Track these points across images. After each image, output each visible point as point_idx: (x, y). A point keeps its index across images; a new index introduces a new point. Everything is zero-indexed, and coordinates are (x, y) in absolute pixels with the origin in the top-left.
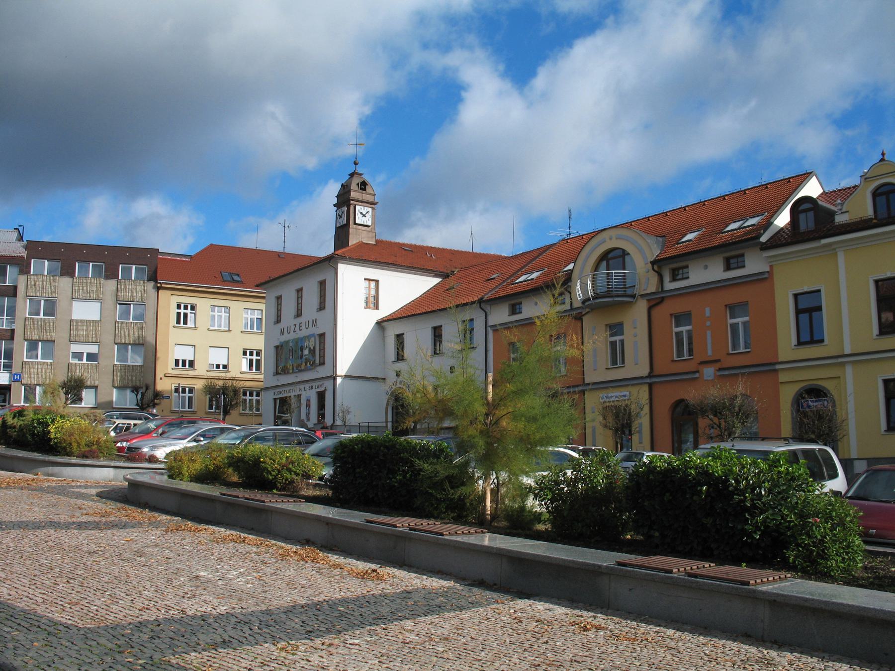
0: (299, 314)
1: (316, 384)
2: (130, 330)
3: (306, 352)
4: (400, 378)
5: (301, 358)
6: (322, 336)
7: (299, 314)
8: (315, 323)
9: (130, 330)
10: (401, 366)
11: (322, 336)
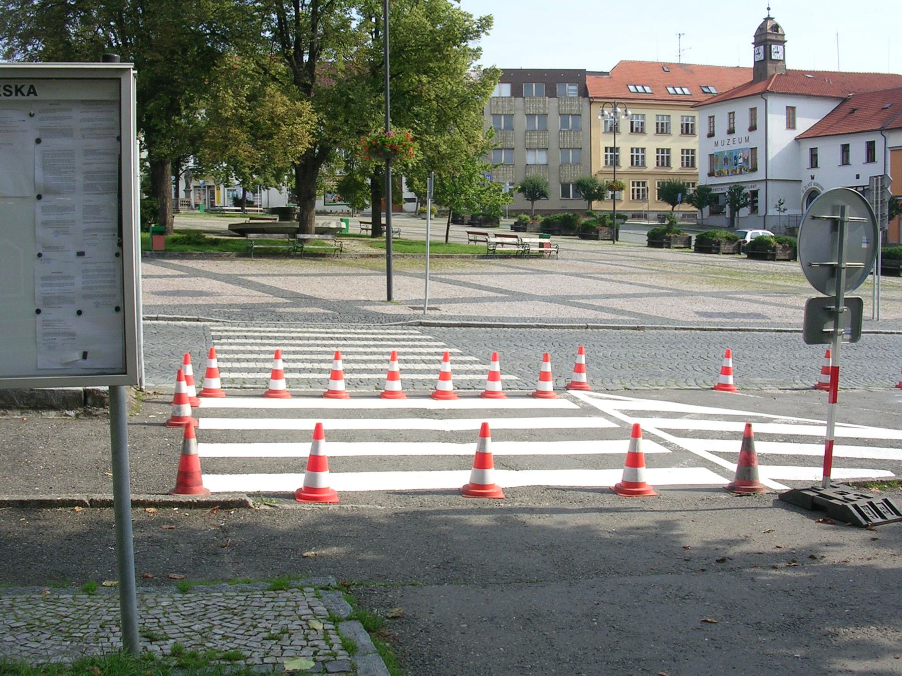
0: (731, 131)
1: (750, 185)
2: (570, 137)
3: (741, 161)
4: (814, 181)
5: (736, 165)
6: (754, 150)
7: (731, 131)
8: (747, 140)
9: (570, 137)
10: (814, 172)
11: (754, 150)
